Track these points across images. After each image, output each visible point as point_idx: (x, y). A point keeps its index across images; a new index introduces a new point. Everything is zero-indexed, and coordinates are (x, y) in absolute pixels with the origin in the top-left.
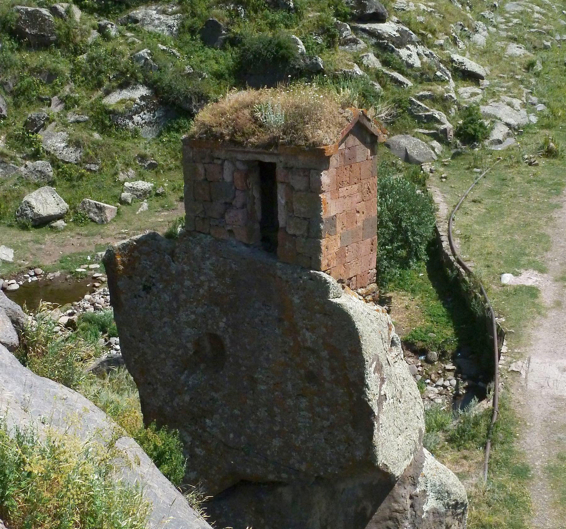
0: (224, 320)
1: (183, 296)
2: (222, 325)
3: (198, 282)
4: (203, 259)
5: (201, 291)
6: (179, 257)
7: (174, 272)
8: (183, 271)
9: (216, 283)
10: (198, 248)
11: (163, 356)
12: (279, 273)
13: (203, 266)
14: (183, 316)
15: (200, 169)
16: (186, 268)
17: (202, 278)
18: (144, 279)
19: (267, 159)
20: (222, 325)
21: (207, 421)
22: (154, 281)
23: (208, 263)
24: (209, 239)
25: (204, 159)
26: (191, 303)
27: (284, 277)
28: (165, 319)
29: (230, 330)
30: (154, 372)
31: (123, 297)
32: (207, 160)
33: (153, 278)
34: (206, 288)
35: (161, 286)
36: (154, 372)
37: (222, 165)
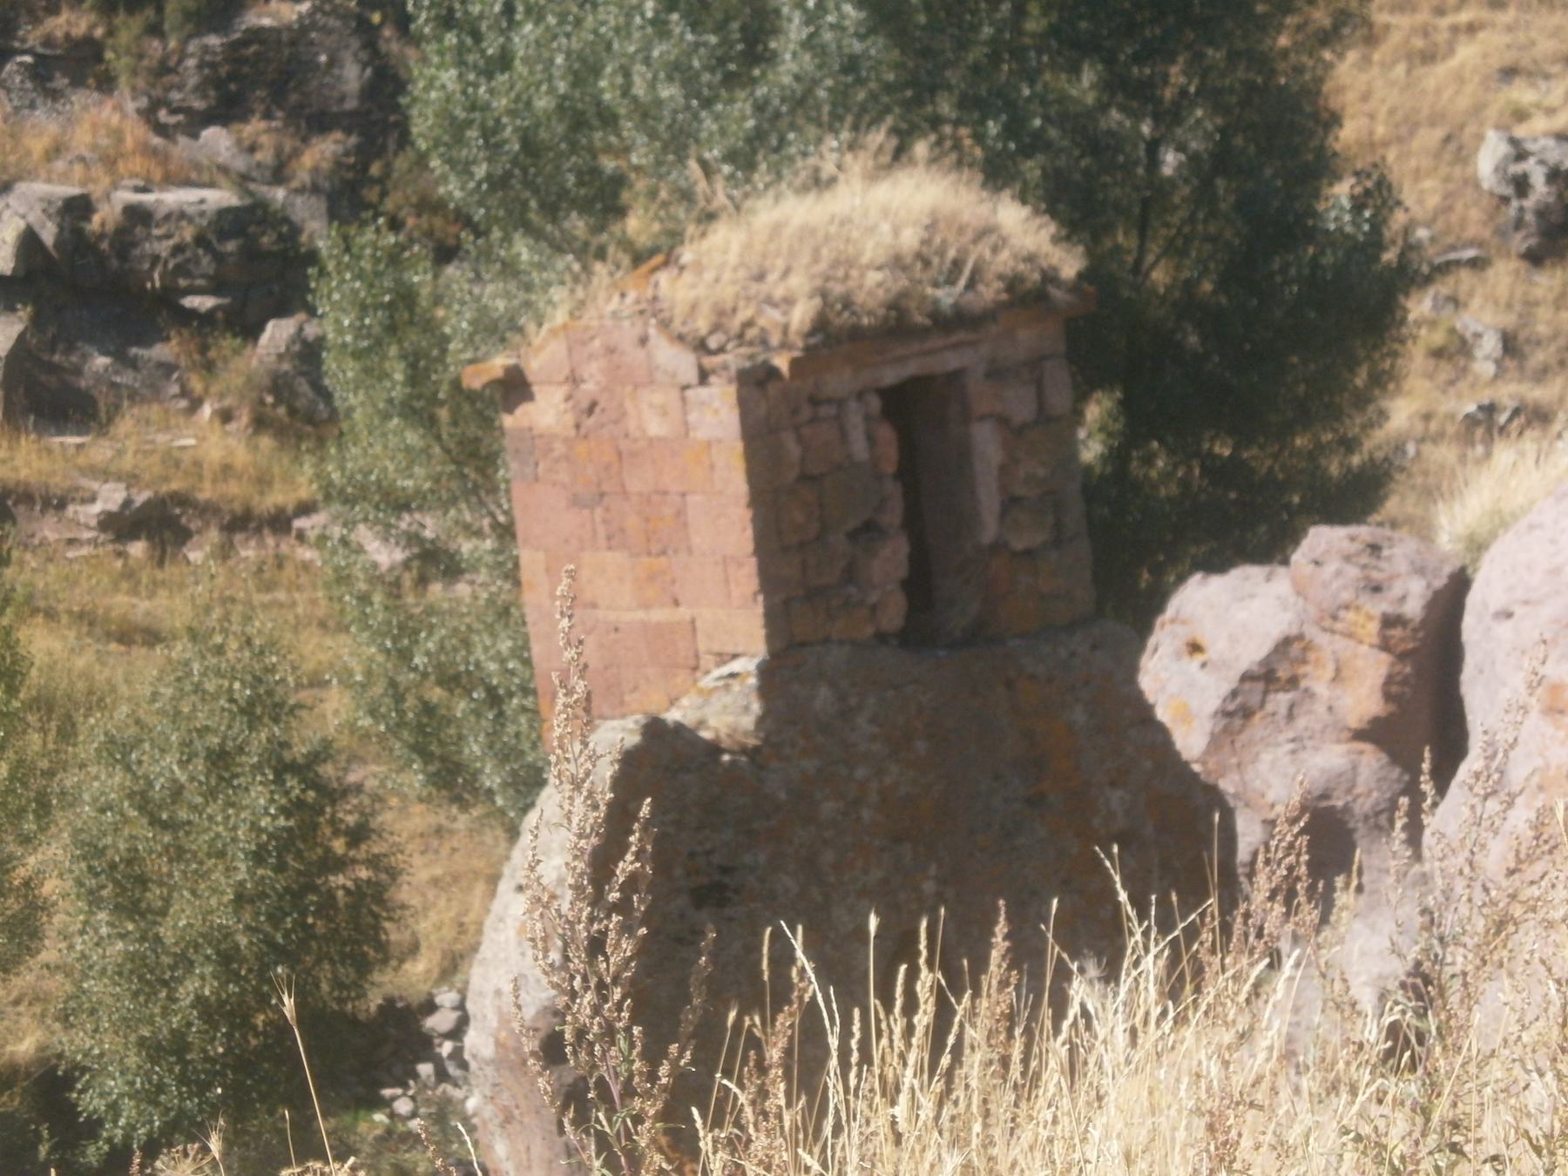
0: (933, 870)
5: (866, 814)
7: (783, 796)
9: (894, 769)
10: (824, 693)
15: (793, 449)
16: (810, 765)
17: (860, 773)
18: (678, 872)
19: (952, 361)
22: (716, 859)
23: (861, 720)
25: (795, 412)
32: (806, 412)
33: (709, 853)
35: (762, 858)
37: (839, 419)
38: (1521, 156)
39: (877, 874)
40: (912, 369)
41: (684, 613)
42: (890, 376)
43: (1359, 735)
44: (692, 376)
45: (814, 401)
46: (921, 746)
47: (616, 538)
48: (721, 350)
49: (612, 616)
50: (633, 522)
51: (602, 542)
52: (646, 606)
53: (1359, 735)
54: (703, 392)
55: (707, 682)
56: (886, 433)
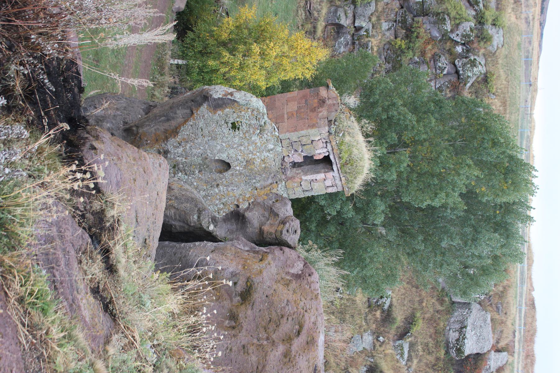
0: (241, 169)
1: (242, 148)
2: (238, 168)
3: (254, 153)
4: (269, 151)
5: (251, 155)
6: (262, 137)
8: (256, 144)
11: (202, 148)
12: (280, 186)
13: (264, 152)
14: (231, 151)
15: (317, 139)
16: (259, 144)
17: (258, 154)
18: (238, 120)
20: (238, 168)
21: (180, 174)
23: (268, 153)
24: (279, 149)
26: (241, 153)
27: (279, 189)
28: (224, 144)
29: (237, 172)
30: (189, 145)
31: (219, 112)
32: (324, 141)
34: (254, 157)
35: (241, 135)
36: (189, 145)
38: (387, 297)
39: (240, 158)
40: (333, 160)
41: (286, 120)
42: (332, 157)
43: (261, 229)
44: (329, 119)
45: (326, 142)
46: (264, 165)
47: (299, 108)
48: (335, 125)
49: (285, 108)
50: (303, 110)
51: (299, 105)
52: (287, 113)
53: (261, 229)
54: (327, 122)
55: (273, 125)
56: (321, 157)
